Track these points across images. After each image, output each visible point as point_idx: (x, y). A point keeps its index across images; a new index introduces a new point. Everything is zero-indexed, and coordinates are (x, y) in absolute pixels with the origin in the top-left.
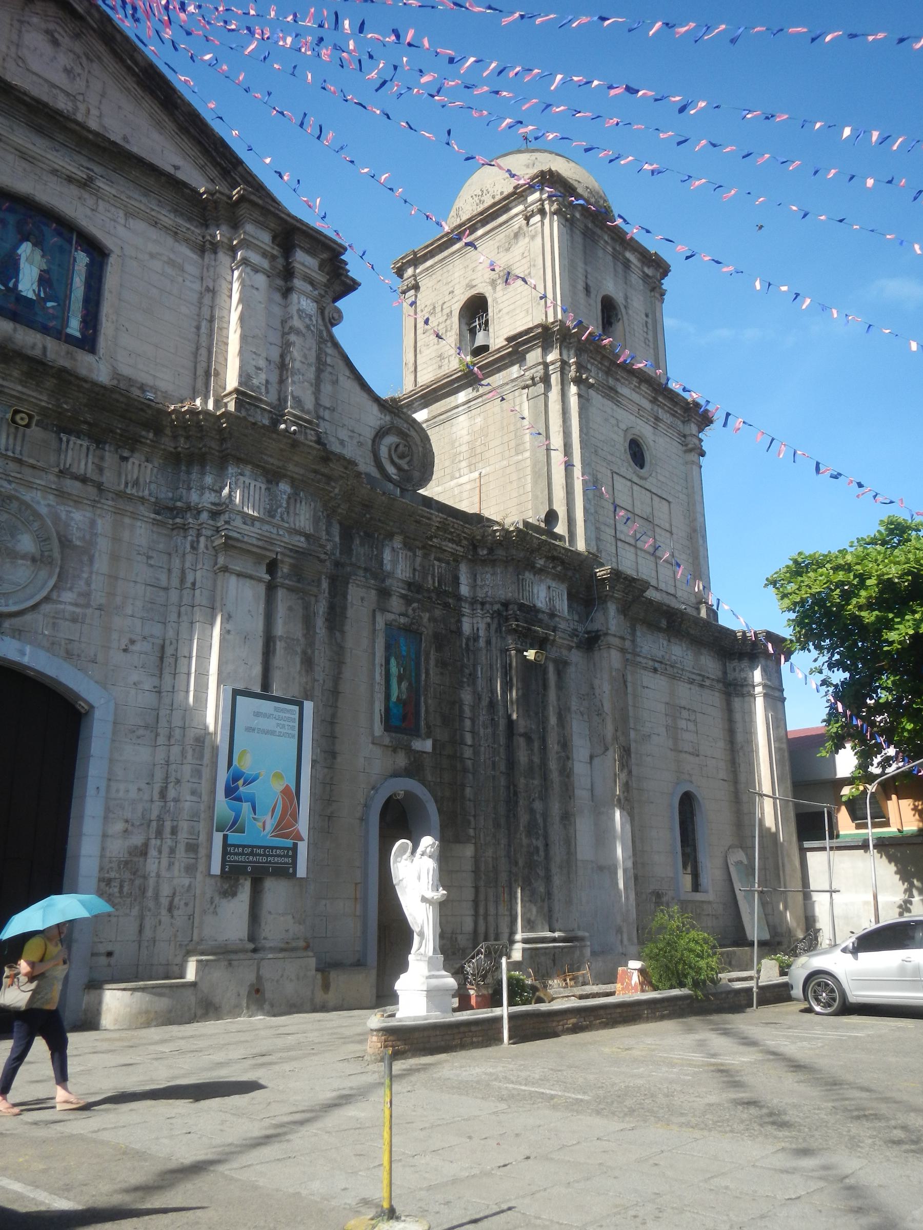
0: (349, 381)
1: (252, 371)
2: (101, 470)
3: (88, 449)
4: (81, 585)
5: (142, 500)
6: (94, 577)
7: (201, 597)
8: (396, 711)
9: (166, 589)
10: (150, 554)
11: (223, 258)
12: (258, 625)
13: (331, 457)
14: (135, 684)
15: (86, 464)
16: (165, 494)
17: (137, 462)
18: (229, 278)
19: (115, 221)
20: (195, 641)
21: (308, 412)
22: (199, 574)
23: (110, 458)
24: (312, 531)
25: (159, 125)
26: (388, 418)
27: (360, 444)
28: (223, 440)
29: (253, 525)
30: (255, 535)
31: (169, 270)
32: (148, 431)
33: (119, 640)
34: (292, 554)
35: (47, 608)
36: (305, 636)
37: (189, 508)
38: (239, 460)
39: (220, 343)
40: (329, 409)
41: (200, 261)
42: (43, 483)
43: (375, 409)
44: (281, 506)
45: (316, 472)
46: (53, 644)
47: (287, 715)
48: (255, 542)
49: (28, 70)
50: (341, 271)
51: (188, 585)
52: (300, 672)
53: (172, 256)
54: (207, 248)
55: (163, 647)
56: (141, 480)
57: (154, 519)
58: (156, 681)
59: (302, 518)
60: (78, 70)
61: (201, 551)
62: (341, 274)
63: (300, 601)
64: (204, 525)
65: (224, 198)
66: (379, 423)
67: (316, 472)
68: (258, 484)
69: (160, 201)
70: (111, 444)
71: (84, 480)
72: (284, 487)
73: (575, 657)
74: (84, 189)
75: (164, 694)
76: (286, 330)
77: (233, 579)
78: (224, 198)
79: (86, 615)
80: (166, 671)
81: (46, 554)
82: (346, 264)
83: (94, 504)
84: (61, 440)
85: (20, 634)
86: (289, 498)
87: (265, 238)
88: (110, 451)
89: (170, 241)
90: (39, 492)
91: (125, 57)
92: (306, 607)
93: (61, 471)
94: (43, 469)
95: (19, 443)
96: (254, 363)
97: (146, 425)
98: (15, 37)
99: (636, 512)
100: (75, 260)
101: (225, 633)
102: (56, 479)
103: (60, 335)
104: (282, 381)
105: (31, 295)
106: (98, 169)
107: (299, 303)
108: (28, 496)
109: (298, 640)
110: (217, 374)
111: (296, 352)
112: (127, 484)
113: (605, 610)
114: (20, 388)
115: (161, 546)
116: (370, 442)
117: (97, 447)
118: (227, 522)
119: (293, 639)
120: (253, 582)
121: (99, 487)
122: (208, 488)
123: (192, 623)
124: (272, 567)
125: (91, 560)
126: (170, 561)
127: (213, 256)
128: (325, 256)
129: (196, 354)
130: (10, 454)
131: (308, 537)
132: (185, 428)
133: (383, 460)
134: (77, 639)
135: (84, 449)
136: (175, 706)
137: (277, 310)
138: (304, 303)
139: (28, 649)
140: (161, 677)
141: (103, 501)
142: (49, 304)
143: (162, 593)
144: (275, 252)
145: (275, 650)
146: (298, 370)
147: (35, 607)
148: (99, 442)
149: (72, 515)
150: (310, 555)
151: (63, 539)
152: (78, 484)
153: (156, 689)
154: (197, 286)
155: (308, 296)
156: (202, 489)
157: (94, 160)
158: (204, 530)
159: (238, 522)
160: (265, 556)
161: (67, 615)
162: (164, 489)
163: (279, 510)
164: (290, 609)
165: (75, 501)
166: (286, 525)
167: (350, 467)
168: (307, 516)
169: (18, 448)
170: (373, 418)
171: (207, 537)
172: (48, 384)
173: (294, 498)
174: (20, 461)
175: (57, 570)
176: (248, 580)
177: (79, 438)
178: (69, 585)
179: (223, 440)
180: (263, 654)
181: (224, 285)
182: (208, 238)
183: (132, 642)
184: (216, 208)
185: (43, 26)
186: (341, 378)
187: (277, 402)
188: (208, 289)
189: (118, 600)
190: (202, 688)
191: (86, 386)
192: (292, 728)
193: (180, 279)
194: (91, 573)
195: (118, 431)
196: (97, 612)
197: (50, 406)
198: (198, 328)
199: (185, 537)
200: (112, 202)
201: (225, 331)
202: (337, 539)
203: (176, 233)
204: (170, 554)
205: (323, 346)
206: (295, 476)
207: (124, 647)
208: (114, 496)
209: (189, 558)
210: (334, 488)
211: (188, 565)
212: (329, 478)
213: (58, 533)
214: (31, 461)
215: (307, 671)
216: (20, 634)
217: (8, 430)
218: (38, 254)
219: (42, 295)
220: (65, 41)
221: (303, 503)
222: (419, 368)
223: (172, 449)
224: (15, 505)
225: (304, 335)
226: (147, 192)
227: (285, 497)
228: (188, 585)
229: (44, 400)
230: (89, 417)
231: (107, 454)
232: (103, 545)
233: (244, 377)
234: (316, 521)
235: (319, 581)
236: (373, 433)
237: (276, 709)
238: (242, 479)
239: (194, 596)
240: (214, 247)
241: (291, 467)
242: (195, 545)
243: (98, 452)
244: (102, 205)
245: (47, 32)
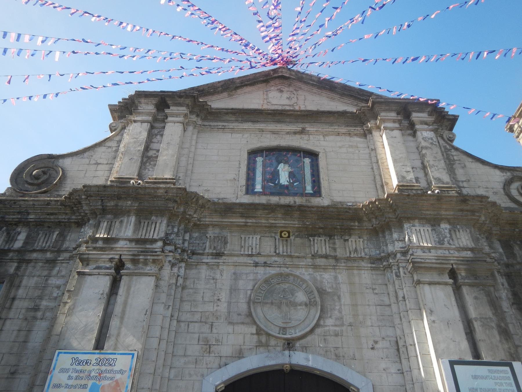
0: (473, 163)
1: (405, 174)
2: (335, 250)
3: (325, 241)
4: (336, 313)
5: (362, 258)
6: (343, 307)
7: (410, 304)
9: (389, 305)
10: (374, 287)
11: (376, 133)
12: (455, 313)
13: (467, 198)
14: (384, 370)
15: (326, 249)
16: (374, 252)
17: (354, 240)
18: (381, 140)
19: (319, 140)
20: (414, 333)
21: (447, 183)
22: (405, 290)
23: (338, 242)
24: (473, 246)
25: (333, 99)
26: (509, 174)
28: (395, 211)
29: (430, 252)
30: (434, 258)
31: (350, 150)
32: (355, 222)
33: (367, 342)
34: (463, 263)
35: (318, 331)
36: (494, 314)
37: (389, 255)
38: (409, 219)
39: (384, 170)
40: (465, 181)
41: (365, 140)
42: (304, 264)
43: (497, 172)
44: (446, 237)
45: (462, 210)
46: (326, 351)
47: (502, 375)
48: (434, 261)
49: (272, 105)
50: (443, 114)
51: (400, 298)
52: (500, 341)
53: (350, 144)
54: (366, 134)
55: (397, 342)
56: (358, 248)
57: (371, 267)
58: (398, 366)
59: (463, 240)
60: (293, 96)
61: (402, 276)
62: (444, 116)
63: (482, 292)
64: (399, 261)
65: (366, 108)
66: (503, 178)
67: (462, 210)
68: (426, 229)
69: (339, 125)
70: (337, 235)
71: (326, 257)
72: (445, 226)
74: (302, 134)
75: (405, 374)
76: (419, 149)
77: (427, 288)
78: (366, 108)
79: (342, 331)
80: (403, 357)
81: (312, 300)
82: (444, 108)
83: (334, 267)
84: (310, 240)
85: (306, 349)
86: (450, 231)
87: (393, 115)
88: (338, 239)
89: (348, 138)
90: (303, 269)
91: (309, 81)
92: (488, 295)
93: (313, 255)
94: (304, 257)
95: (289, 247)
96: (404, 170)
97: (352, 219)
98: (265, 97)
100: (304, 162)
101: (432, 323)
102: (311, 260)
103: (303, 194)
104: (426, 174)
105: (286, 183)
107: (422, 135)
108: (297, 272)
109: (490, 318)
110: (387, 184)
111: (429, 159)
112: (350, 253)
114: (283, 222)
115: (380, 281)
116: (502, 191)
117: (330, 238)
118: (412, 255)
119: (486, 318)
120: (441, 286)
121: (336, 258)
122: (396, 240)
123: (410, 322)
124: (453, 274)
125: (339, 298)
126: (387, 288)
127: (371, 135)
128: (429, 109)
129: (375, 180)
130: (285, 254)
131: (472, 250)
132: (372, 213)
133: (516, 197)
134: (340, 346)
135: (323, 241)
136: (414, 381)
137: (413, 144)
138: (426, 134)
139: (310, 357)
140: (401, 362)
141: (338, 264)
142: (295, 184)
143: (387, 308)
144: (399, 118)
145: (474, 328)
146: (433, 165)
147: (312, 331)
148: (331, 236)
149: (323, 276)
150: (478, 261)
151: (321, 290)
152: (324, 260)
153: (400, 372)
154: (367, 151)
155: (426, 130)
157: (304, 122)
158: (400, 264)
159: (419, 253)
160: (447, 268)
161: (332, 333)
162: (373, 250)
163: (446, 240)
164: (476, 298)
165: (324, 269)
166: (454, 247)
167: (484, 200)
168: (467, 238)
169: (289, 250)
170: (499, 177)
171: (403, 267)
172: (296, 215)
173: (453, 229)
174: (291, 256)
175: (319, 307)
176: (437, 285)
177: (320, 237)
178: (329, 315)
179: (395, 211)
180: (467, 334)
181: (379, 144)
182: (365, 128)
183: (376, 342)
184: (365, 115)
185: (276, 88)
186: (467, 164)
187: (428, 186)
188: (372, 150)
189: (361, 318)
190: (428, 364)
191: (313, 209)
192: (510, 384)
193: (357, 152)
194: (341, 305)
195: (338, 227)
196: (349, 328)
197: (300, 226)
198: (372, 168)
199: (392, 272)
200: (316, 134)
201: (385, 164)
202: (501, 250)
203: (349, 134)
204: (386, 285)
205: (449, 153)
206: (448, 217)
207: (372, 347)
208: (345, 261)
209: (397, 282)
210: (480, 216)
211: (397, 287)
212: (473, 212)
213: (317, 288)
214: (296, 254)
215: (506, 340)
216: (306, 349)
217: (283, 243)
218: (287, 167)
219: (291, 181)
221: (461, 231)
223: (371, 228)
224: (291, 278)
225: (431, 148)
226: (331, 124)
227: (447, 231)
228: (400, 298)
229: (296, 223)
230: (321, 225)
231: (337, 240)
232: (344, 289)
233: (401, 178)
234: (476, 240)
235: (493, 275)
236: (502, 185)
237: (489, 371)
238: (414, 228)
239: (406, 304)
240: (370, 132)
241: (443, 213)
242: (398, 274)
243: (331, 241)
244: (311, 136)
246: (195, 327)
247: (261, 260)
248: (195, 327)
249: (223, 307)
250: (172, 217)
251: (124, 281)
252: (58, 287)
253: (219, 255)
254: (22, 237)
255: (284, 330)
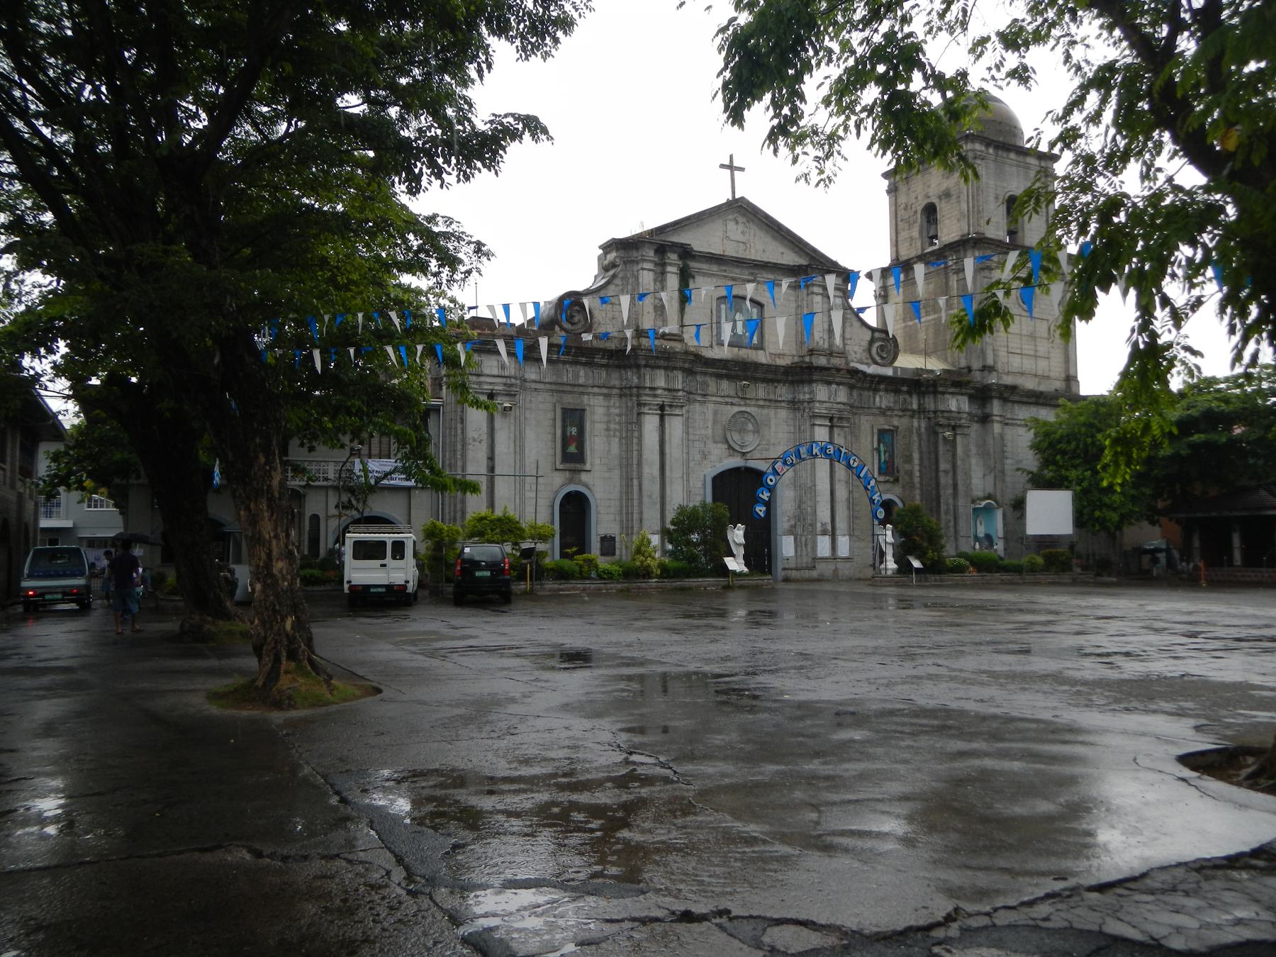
8: (883, 466)
16: (790, 397)
27: (864, 351)
73: (975, 427)
77: (817, 428)
99: (1024, 332)
106: (757, 272)
113: (992, 405)
124: (831, 419)
156: (804, 393)
170: (867, 335)
220: (741, 219)
222: (900, 243)
232: (773, 422)
245: (735, 219)
246: (696, 444)
247: (729, 400)
248: (696, 444)
249: (710, 431)
250: (684, 370)
251: (667, 417)
252: (620, 415)
253: (705, 395)
254: (582, 373)
255: (742, 447)
